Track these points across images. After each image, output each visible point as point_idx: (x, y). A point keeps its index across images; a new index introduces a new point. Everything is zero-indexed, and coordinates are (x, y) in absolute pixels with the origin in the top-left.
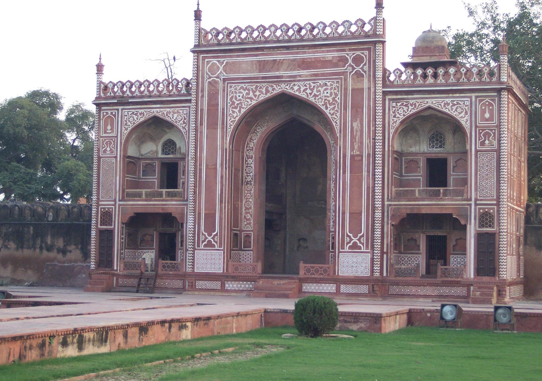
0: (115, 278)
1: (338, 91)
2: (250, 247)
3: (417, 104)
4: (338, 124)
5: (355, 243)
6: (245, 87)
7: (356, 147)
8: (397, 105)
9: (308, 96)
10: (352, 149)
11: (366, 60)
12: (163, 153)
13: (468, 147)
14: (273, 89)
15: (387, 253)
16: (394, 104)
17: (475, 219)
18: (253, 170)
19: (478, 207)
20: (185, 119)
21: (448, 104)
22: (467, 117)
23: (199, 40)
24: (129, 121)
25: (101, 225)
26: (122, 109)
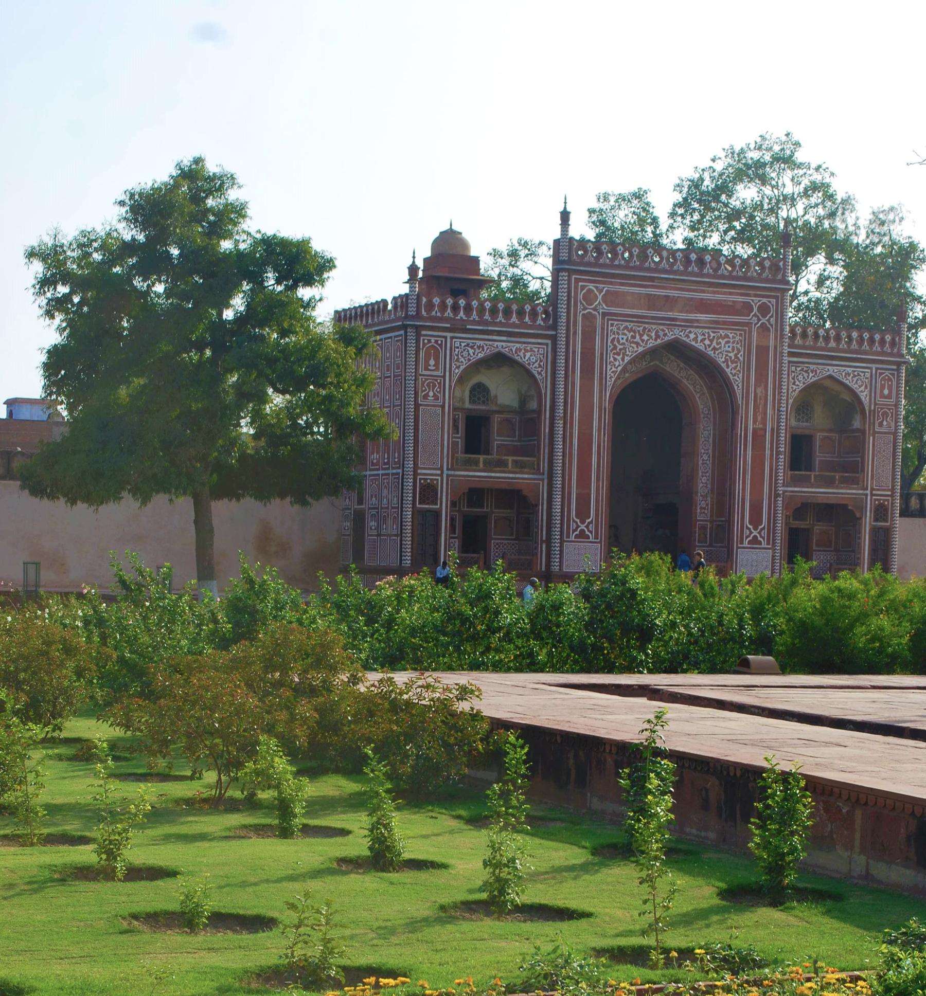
5: (755, 537)
7: (759, 418)
10: (755, 422)
11: (773, 311)
14: (665, 335)
20: (541, 361)
26: (452, 338)
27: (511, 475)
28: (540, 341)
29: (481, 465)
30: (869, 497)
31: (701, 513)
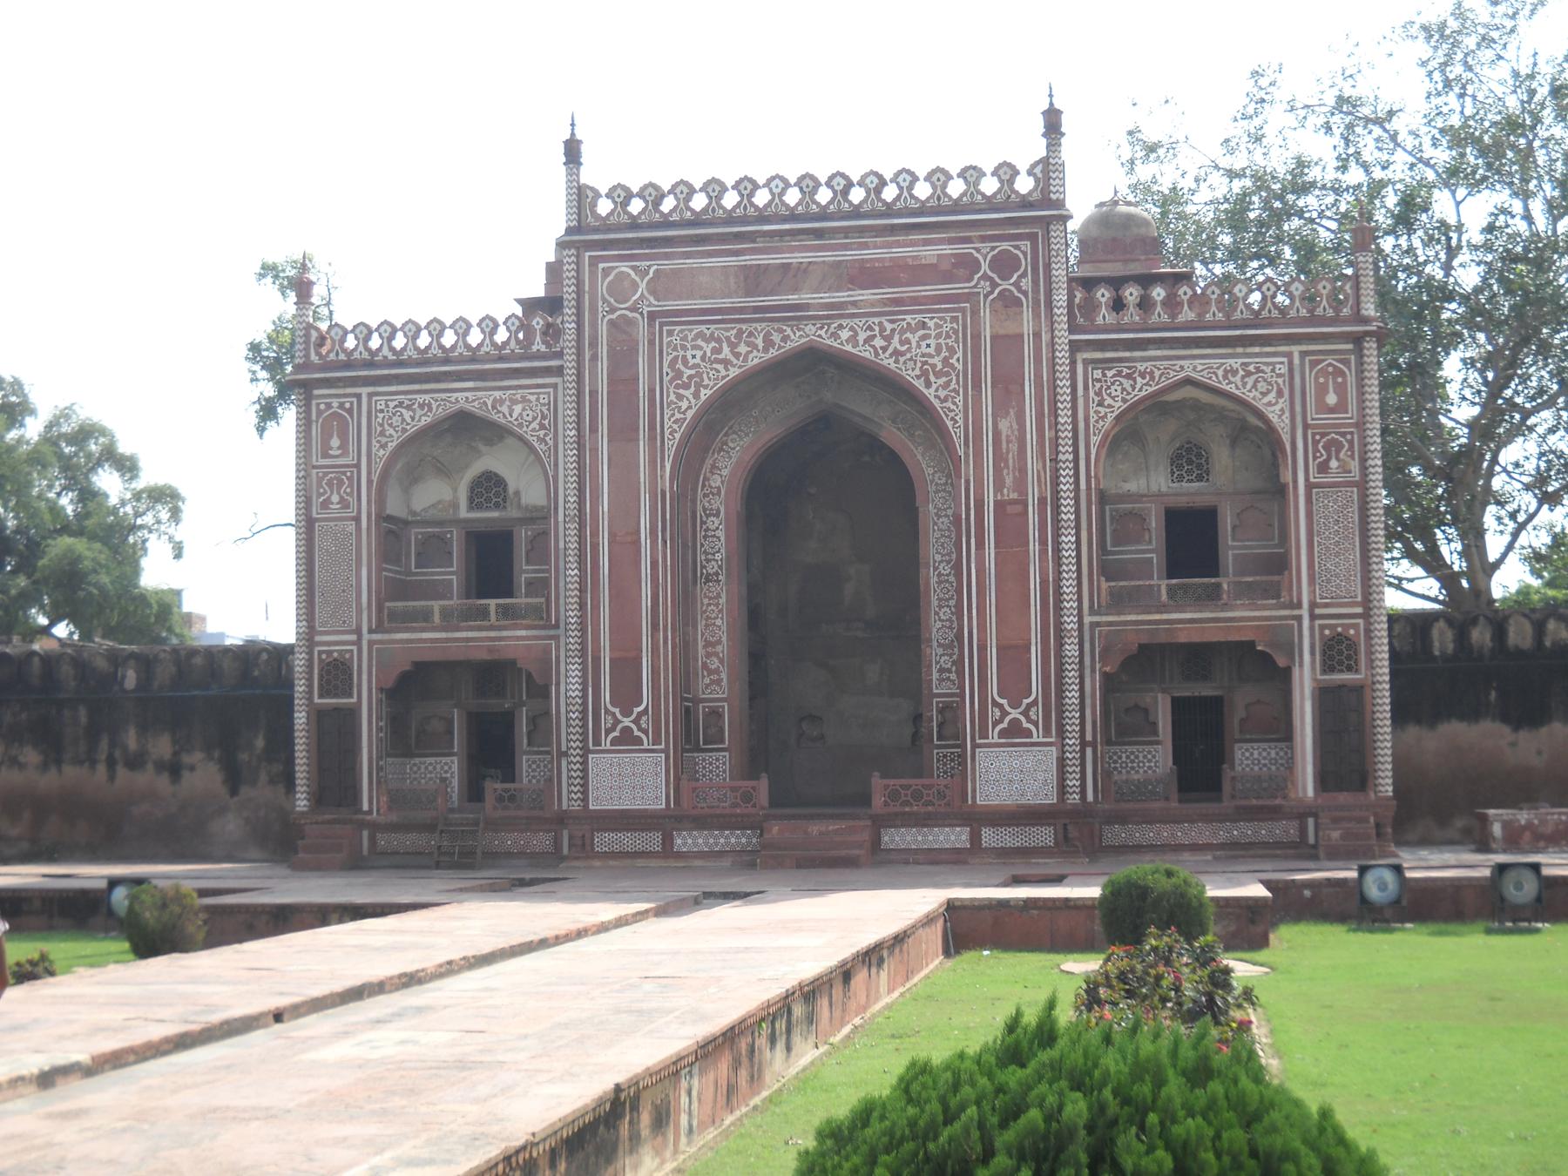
0: (365, 834)
1: (957, 342)
2: (722, 742)
3: (1157, 374)
4: (961, 422)
5: (1015, 722)
6: (708, 333)
7: (1009, 480)
8: (1104, 375)
9: (877, 354)
12: (471, 508)
13: (1287, 477)
14: (785, 339)
15: (1094, 745)
16: (1098, 374)
17: (1312, 653)
18: (722, 544)
19: (1318, 622)
20: (544, 417)
21: (1235, 373)
22: (1283, 403)
23: (579, 215)
24: (390, 425)
25: (321, 696)
26: (370, 395)
27: (493, 634)
28: (540, 381)
29: (437, 618)
30: (1306, 623)
31: (941, 680)
